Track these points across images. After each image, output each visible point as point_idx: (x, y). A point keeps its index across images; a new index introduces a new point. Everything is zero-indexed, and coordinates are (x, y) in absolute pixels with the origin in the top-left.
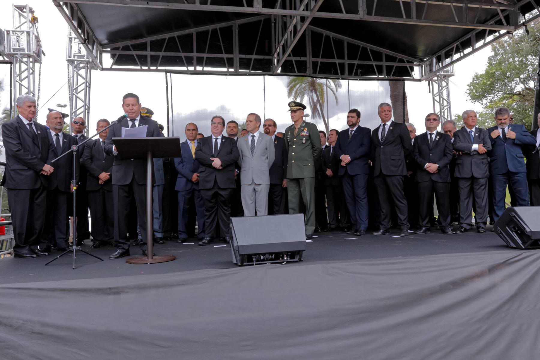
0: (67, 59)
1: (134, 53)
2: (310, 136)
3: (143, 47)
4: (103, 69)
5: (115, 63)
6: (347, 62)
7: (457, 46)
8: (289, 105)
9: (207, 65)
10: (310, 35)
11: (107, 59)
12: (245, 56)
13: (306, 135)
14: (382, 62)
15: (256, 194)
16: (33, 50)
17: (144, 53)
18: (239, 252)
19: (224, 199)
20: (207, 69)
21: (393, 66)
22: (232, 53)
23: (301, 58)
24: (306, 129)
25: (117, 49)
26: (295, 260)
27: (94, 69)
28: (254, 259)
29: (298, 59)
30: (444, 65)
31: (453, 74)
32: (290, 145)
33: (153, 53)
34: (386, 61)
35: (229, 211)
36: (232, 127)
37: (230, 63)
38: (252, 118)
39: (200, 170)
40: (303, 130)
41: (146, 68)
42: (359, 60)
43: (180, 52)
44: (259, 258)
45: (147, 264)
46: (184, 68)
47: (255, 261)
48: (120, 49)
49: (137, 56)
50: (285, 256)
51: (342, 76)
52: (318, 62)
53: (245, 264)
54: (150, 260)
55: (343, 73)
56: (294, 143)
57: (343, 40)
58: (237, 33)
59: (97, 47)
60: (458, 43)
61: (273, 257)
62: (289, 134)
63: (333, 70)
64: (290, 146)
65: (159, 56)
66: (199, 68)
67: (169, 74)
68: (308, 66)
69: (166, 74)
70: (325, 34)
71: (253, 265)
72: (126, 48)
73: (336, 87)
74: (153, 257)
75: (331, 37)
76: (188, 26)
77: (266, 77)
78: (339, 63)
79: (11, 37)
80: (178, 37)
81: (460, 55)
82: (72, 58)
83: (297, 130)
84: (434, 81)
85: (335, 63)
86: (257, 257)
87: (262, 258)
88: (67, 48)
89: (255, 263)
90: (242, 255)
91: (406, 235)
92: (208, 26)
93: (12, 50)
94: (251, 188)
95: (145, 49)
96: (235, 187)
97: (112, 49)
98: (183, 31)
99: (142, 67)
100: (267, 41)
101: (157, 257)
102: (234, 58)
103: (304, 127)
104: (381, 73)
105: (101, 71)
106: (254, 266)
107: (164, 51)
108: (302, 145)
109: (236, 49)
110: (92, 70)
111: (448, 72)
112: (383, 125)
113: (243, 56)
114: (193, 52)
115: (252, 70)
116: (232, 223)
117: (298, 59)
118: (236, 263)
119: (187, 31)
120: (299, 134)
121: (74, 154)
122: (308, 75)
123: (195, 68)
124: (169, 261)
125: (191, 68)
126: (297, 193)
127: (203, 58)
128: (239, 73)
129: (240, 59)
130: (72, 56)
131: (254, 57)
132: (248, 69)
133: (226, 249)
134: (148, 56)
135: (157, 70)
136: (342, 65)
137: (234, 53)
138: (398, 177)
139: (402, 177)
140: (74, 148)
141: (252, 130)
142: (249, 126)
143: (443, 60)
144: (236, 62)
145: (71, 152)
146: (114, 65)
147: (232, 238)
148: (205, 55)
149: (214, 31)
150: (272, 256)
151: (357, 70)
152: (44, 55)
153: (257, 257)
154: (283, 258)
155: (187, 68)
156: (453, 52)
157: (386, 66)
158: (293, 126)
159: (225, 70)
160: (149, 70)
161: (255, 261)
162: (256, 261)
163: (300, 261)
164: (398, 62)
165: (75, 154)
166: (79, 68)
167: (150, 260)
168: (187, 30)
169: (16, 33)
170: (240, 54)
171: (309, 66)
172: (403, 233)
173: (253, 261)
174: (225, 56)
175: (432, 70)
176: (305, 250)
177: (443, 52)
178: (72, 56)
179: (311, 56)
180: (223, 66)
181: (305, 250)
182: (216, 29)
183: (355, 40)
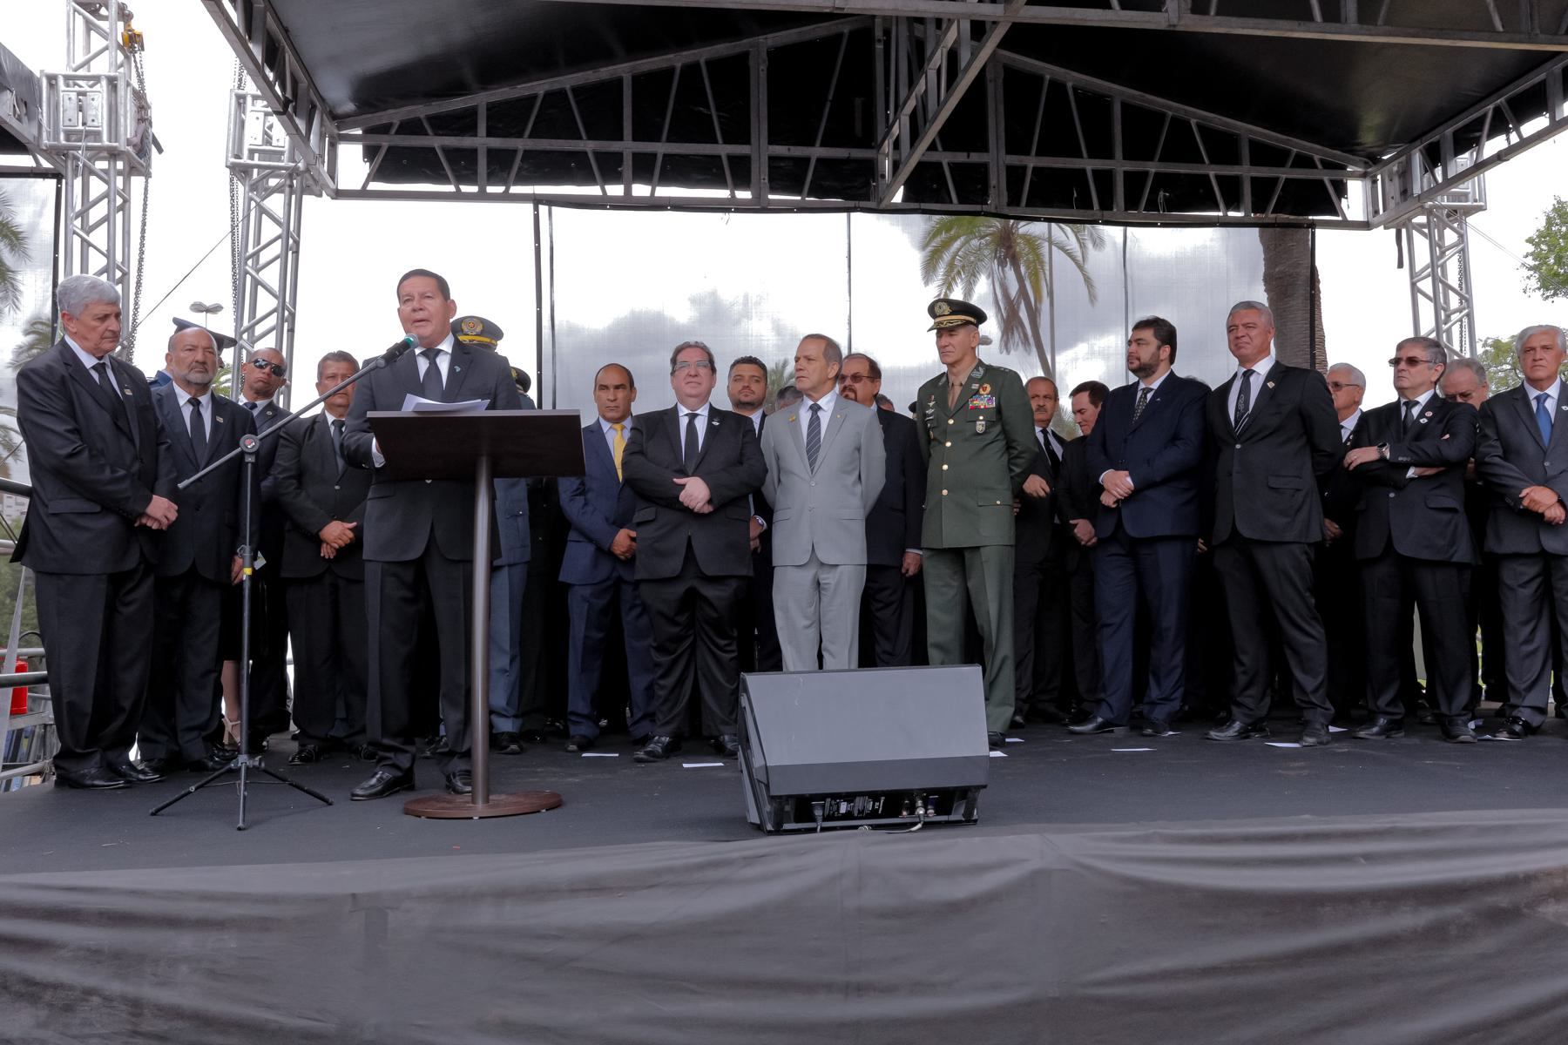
0: (229, 164)
1: (437, 142)
2: (999, 410)
3: (463, 123)
4: (339, 194)
5: (377, 175)
6: (1120, 166)
7: (1497, 110)
8: (932, 310)
9: (668, 178)
10: (1000, 81)
11: (352, 163)
12: (789, 149)
13: (988, 406)
14: (1236, 167)
15: (823, 598)
16: (126, 134)
17: (466, 142)
18: (767, 786)
19: (715, 615)
20: (664, 192)
21: (1275, 180)
22: (747, 141)
23: (968, 157)
25: (384, 129)
26: (953, 817)
27: (311, 193)
28: (818, 813)
29: (961, 157)
30: (1450, 175)
31: (1482, 204)
32: (935, 439)
33: (496, 142)
34: (1254, 163)
35: (732, 651)
36: (747, 378)
37: (740, 174)
38: (814, 350)
39: (638, 518)
41: (474, 189)
42: (1159, 161)
43: (580, 138)
44: (835, 808)
45: (472, 818)
46: (594, 190)
47: (820, 819)
48: (394, 130)
49: (447, 151)
50: (920, 803)
51: (1106, 213)
52: (1024, 168)
53: (787, 826)
54: (480, 807)
55: (1106, 204)
56: (946, 433)
57: (1110, 96)
58: (763, 75)
59: (322, 124)
60: (1499, 101)
61: (880, 805)
62: (931, 404)
63: (1075, 195)
64: (933, 443)
65: (515, 151)
66: (641, 190)
67: (543, 209)
68: (993, 182)
69: (536, 209)
70: (1048, 77)
71: (813, 830)
72: (411, 127)
73: (1081, 247)
74: (491, 797)
75: (1069, 85)
76: (608, 57)
77: (855, 216)
78: (1094, 171)
79: (61, 94)
80: (574, 90)
81: (1508, 139)
82: (245, 160)
83: (958, 390)
84: (1414, 228)
85: (1083, 171)
86: (827, 805)
87: (844, 808)
88: (229, 130)
89: (820, 824)
90: (780, 797)
91: (1320, 743)
92: (672, 56)
93: (62, 136)
94: (807, 576)
95: (471, 130)
96: (751, 574)
97: (367, 131)
98: (590, 72)
99: (461, 186)
100: (858, 101)
101: (503, 797)
102: (754, 158)
103: (981, 381)
104: (1236, 204)
105: (332, 199)
106: (818, 835)
107: (531, 136)
108: (974, 438)
109: (760, 126)
110: (306, 198)
111: (1465, 196)
112: (1244, 374)
113: (780, 150)
114: (621, 139)
115: (809, 196)
116: (746, 691)
117: (961, 157)
118: (759, 822)
119: (605, 73)
120: (962, 405)
121: (248, 463)
122: (994, 211)
123: (628, 190)
124: (539, 812)
125: (616, 190)
126: (956, 595)
127: (654, 155)
128: (769, 204)
129: (772, 159)
130: (246, 153)
131: (817, 152)
132: (799, 193)
133: (725, 774)
134: (479, 151)
135: (506, 197)
136: (1104, 178)
137: (753, 140)
138: (1295, 548)
139: (1306, 546)
140: (250, 443)
141: (814, 388)
142: (801, 373)
143: (1448, 157)
144: (760, 170)
145: (237, 455)
146: (374, 180)
147: (748, 740)
148: (661, 148)
149: (691, 70)
150: (877, 804)
151: (1154, 192)
152: (160, 150)
153: (827, 805)
154: (912, 810)
155: (604, 191)
156: (1481, 130)
157: (1253, 179)
158: (944, 379)
159: (723, 194)
160: (482, 197)
161: (820, 819)
162: (825, 819)
163: (969, 821)
164: (1291, 167)
165: (252, 463)
166: (266, 189)
167: (480, 807)
168: (602, 70)
169: (75, 84)
170: (771, 142)
171: (997, 181)
172: (1311, 736)
173: (813, 819)
174: (723, 150)
175: (1409, 192)
176: (985, 787)
177: (1449, 131)
178: (246, 153)
179: (1003, 150)
180: (719, 182)
181: (985, 787)
182: (696, 65)
183: (1148, 96)
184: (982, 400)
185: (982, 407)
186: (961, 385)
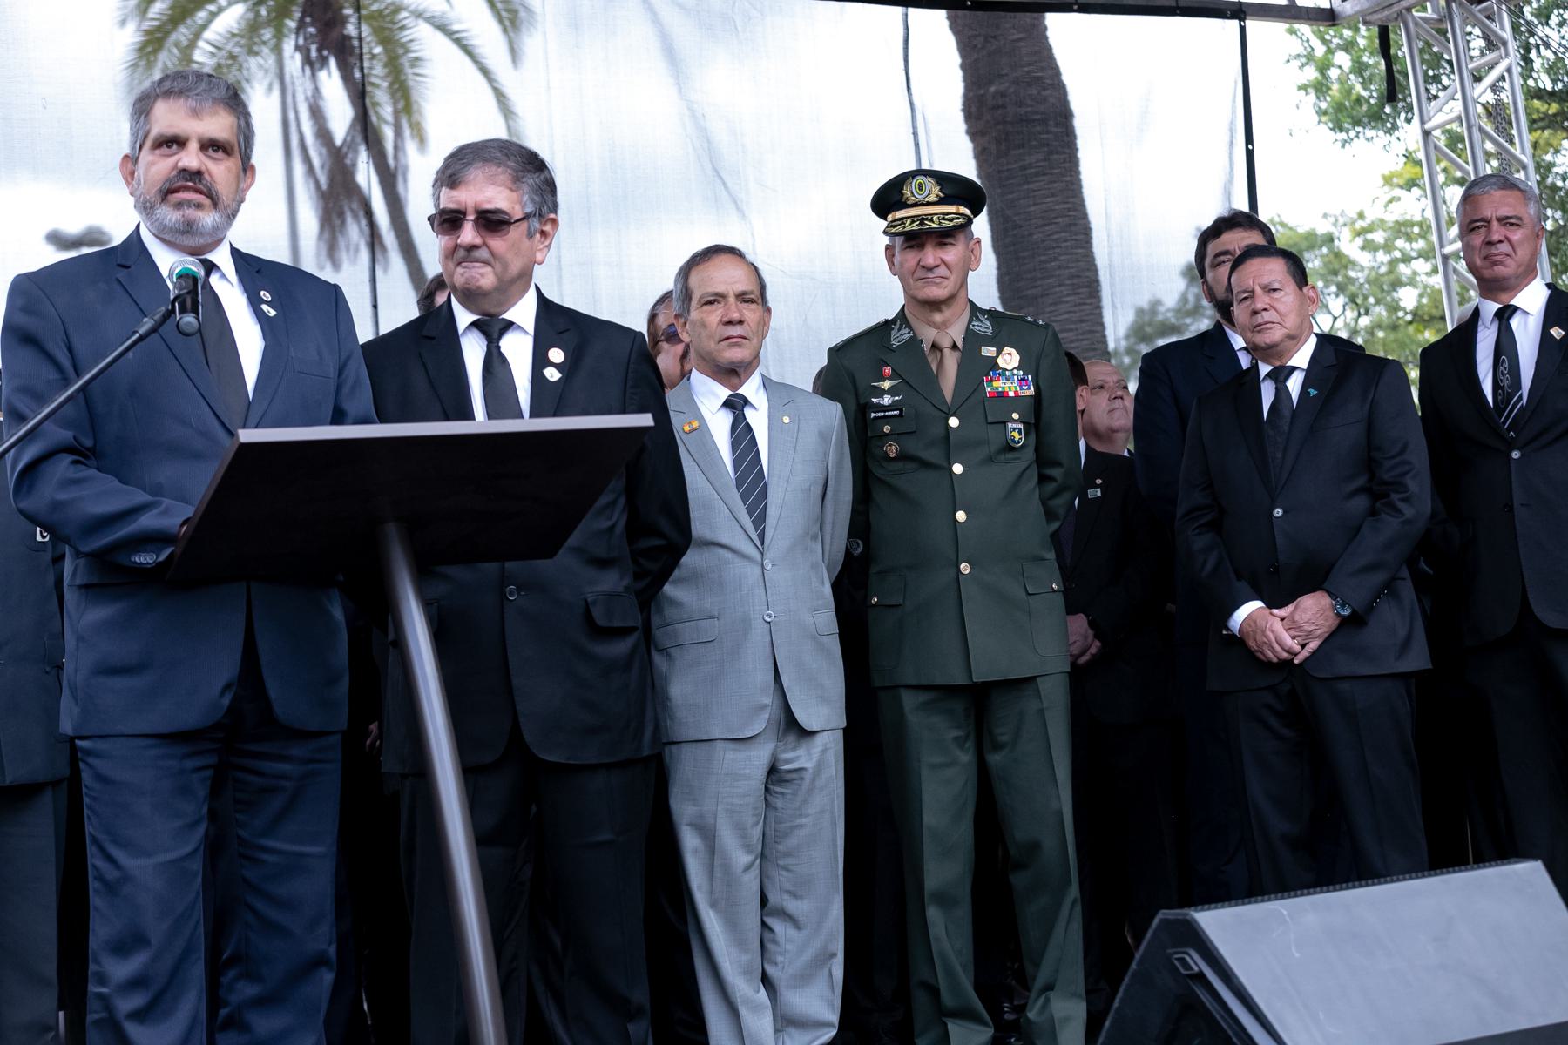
24: (1013, 351)
40: (992, 364)
184: (1007, 379)
185: (1011, 394)
186: (954, 347)
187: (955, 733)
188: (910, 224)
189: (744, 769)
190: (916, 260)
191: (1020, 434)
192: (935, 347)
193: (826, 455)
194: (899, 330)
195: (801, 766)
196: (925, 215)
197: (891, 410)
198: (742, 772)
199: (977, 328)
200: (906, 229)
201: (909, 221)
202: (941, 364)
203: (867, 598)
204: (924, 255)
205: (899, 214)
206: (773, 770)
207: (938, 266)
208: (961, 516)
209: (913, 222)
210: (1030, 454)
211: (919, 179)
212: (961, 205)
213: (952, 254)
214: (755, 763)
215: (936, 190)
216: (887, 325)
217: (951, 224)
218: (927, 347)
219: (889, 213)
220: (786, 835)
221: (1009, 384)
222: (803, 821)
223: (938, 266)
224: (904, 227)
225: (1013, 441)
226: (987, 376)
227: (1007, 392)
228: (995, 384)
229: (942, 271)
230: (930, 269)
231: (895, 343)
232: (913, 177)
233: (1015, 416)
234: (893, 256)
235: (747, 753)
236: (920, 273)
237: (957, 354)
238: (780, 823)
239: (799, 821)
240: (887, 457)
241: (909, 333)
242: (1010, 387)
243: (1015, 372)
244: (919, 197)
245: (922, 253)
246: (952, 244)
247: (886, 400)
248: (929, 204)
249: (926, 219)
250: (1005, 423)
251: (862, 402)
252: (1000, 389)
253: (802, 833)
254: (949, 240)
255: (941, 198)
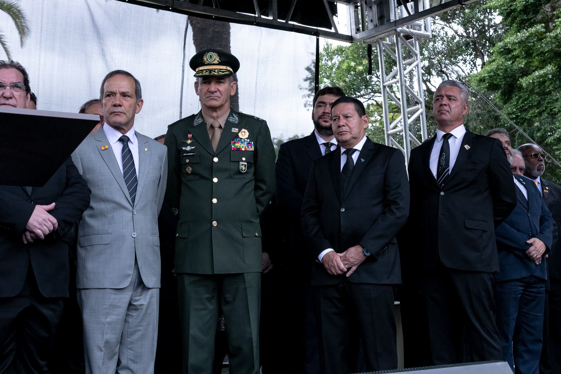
24: (246, 131)
40: (236, 136)
56: (212, 170)
83: (218, 133)
103: (240, 126)
108: (236, 176)
184: (242, 143)
185: (243, 149)
186: (220, 127)
187: (207, 296)
188: (205, 73)
189: (119, 303)
190: (207, 89)
191: (245, 167)
192: (212, 127)
193: (161, 168)
194: (198, 119)
195: (142, 303)
196: (212, 69)
197: (190, 153)
198: (117, 304)
199: (232, 120)
200: (203, 74)
201: (205, 71)
202: (213, 135)
203: (176, 234)
204: (211, 86)
205: (201, 68)
206: (130, 304)
207: (216, 92)
208: (215, 201)
209: (206, 72)
210: (250, 176)
211: (211, 53)
212: (228, 66)
213: (223, 87)
214: (123, 300)
215: (218, 59)
216: (193, 116)
217: (223, 74)
218: (208, 126)
219: (197, 68)
220: (133, 334)
221: (242, 145)
222: (141, 328)
223: (216, 92)
224: (203, 74)
225: (242, 170)
226: (233, 140)
227: (242, 148)
228: (236, 144)
229: (218, 94)
230: (213, 93)
231: (195, 124)
232: (208, 52)
233: (244, 159)
234: (198, 87)
235: (120, 296)
236: (208, 95)
237: (222, 130)
238: (131, 329)
239: (139, 328)
240: (187, 173)
241: (202, 120)
242: (243, 146)
243: (246, 140)
244: (210, 61)
245: (209, 86)
246: (223, 82)
247: (188, 148)
248: (214, 64)
249: (212, 71)
250: (238, 162)
251: (179, 149)
252: (238, 147)
253: (139, 334)
254: (222, 81)
255: (219, 62)
